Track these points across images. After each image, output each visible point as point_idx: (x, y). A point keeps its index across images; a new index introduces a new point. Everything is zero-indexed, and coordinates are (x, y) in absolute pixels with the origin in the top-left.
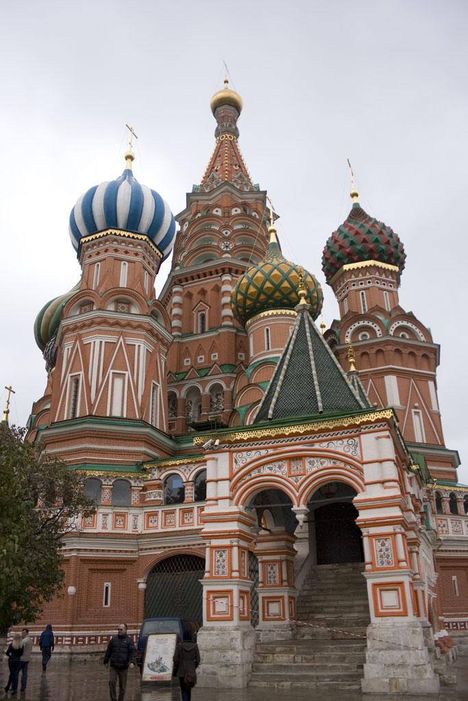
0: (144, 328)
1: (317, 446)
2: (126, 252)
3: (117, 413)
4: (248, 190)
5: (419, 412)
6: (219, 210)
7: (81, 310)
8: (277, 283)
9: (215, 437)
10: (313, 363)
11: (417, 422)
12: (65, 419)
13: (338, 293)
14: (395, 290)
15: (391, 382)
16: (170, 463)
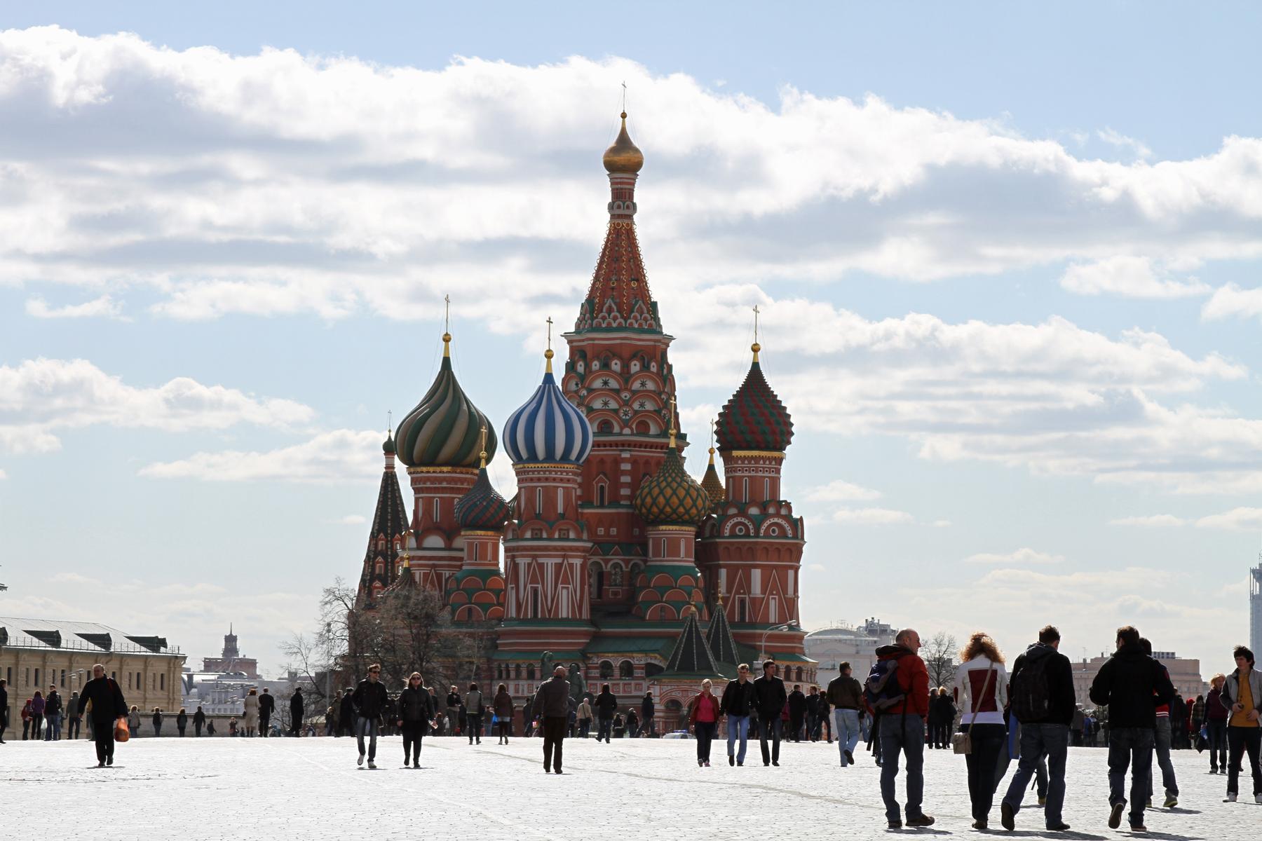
0: (580, 551)
1: (693, 687)
2: (562, 480)
3: (564, 615)
4: (646, 327)
5: (775, 598)
6: (618, 362)
7: (532, 535)
8: (675, 508)
9: (655, 680)
10: (695, 646)
11: (773, 605)
12: (529, 617)
13: (728, 468)
14: (776, 475)
15: (757, 574)
16: (607, 655)
